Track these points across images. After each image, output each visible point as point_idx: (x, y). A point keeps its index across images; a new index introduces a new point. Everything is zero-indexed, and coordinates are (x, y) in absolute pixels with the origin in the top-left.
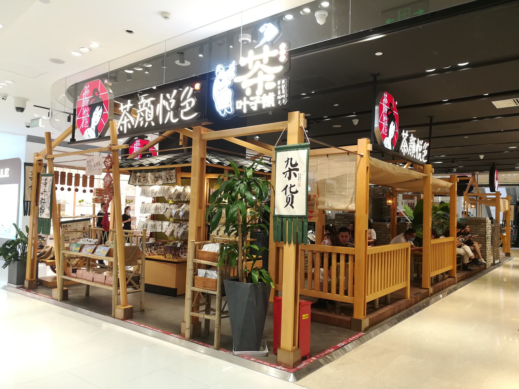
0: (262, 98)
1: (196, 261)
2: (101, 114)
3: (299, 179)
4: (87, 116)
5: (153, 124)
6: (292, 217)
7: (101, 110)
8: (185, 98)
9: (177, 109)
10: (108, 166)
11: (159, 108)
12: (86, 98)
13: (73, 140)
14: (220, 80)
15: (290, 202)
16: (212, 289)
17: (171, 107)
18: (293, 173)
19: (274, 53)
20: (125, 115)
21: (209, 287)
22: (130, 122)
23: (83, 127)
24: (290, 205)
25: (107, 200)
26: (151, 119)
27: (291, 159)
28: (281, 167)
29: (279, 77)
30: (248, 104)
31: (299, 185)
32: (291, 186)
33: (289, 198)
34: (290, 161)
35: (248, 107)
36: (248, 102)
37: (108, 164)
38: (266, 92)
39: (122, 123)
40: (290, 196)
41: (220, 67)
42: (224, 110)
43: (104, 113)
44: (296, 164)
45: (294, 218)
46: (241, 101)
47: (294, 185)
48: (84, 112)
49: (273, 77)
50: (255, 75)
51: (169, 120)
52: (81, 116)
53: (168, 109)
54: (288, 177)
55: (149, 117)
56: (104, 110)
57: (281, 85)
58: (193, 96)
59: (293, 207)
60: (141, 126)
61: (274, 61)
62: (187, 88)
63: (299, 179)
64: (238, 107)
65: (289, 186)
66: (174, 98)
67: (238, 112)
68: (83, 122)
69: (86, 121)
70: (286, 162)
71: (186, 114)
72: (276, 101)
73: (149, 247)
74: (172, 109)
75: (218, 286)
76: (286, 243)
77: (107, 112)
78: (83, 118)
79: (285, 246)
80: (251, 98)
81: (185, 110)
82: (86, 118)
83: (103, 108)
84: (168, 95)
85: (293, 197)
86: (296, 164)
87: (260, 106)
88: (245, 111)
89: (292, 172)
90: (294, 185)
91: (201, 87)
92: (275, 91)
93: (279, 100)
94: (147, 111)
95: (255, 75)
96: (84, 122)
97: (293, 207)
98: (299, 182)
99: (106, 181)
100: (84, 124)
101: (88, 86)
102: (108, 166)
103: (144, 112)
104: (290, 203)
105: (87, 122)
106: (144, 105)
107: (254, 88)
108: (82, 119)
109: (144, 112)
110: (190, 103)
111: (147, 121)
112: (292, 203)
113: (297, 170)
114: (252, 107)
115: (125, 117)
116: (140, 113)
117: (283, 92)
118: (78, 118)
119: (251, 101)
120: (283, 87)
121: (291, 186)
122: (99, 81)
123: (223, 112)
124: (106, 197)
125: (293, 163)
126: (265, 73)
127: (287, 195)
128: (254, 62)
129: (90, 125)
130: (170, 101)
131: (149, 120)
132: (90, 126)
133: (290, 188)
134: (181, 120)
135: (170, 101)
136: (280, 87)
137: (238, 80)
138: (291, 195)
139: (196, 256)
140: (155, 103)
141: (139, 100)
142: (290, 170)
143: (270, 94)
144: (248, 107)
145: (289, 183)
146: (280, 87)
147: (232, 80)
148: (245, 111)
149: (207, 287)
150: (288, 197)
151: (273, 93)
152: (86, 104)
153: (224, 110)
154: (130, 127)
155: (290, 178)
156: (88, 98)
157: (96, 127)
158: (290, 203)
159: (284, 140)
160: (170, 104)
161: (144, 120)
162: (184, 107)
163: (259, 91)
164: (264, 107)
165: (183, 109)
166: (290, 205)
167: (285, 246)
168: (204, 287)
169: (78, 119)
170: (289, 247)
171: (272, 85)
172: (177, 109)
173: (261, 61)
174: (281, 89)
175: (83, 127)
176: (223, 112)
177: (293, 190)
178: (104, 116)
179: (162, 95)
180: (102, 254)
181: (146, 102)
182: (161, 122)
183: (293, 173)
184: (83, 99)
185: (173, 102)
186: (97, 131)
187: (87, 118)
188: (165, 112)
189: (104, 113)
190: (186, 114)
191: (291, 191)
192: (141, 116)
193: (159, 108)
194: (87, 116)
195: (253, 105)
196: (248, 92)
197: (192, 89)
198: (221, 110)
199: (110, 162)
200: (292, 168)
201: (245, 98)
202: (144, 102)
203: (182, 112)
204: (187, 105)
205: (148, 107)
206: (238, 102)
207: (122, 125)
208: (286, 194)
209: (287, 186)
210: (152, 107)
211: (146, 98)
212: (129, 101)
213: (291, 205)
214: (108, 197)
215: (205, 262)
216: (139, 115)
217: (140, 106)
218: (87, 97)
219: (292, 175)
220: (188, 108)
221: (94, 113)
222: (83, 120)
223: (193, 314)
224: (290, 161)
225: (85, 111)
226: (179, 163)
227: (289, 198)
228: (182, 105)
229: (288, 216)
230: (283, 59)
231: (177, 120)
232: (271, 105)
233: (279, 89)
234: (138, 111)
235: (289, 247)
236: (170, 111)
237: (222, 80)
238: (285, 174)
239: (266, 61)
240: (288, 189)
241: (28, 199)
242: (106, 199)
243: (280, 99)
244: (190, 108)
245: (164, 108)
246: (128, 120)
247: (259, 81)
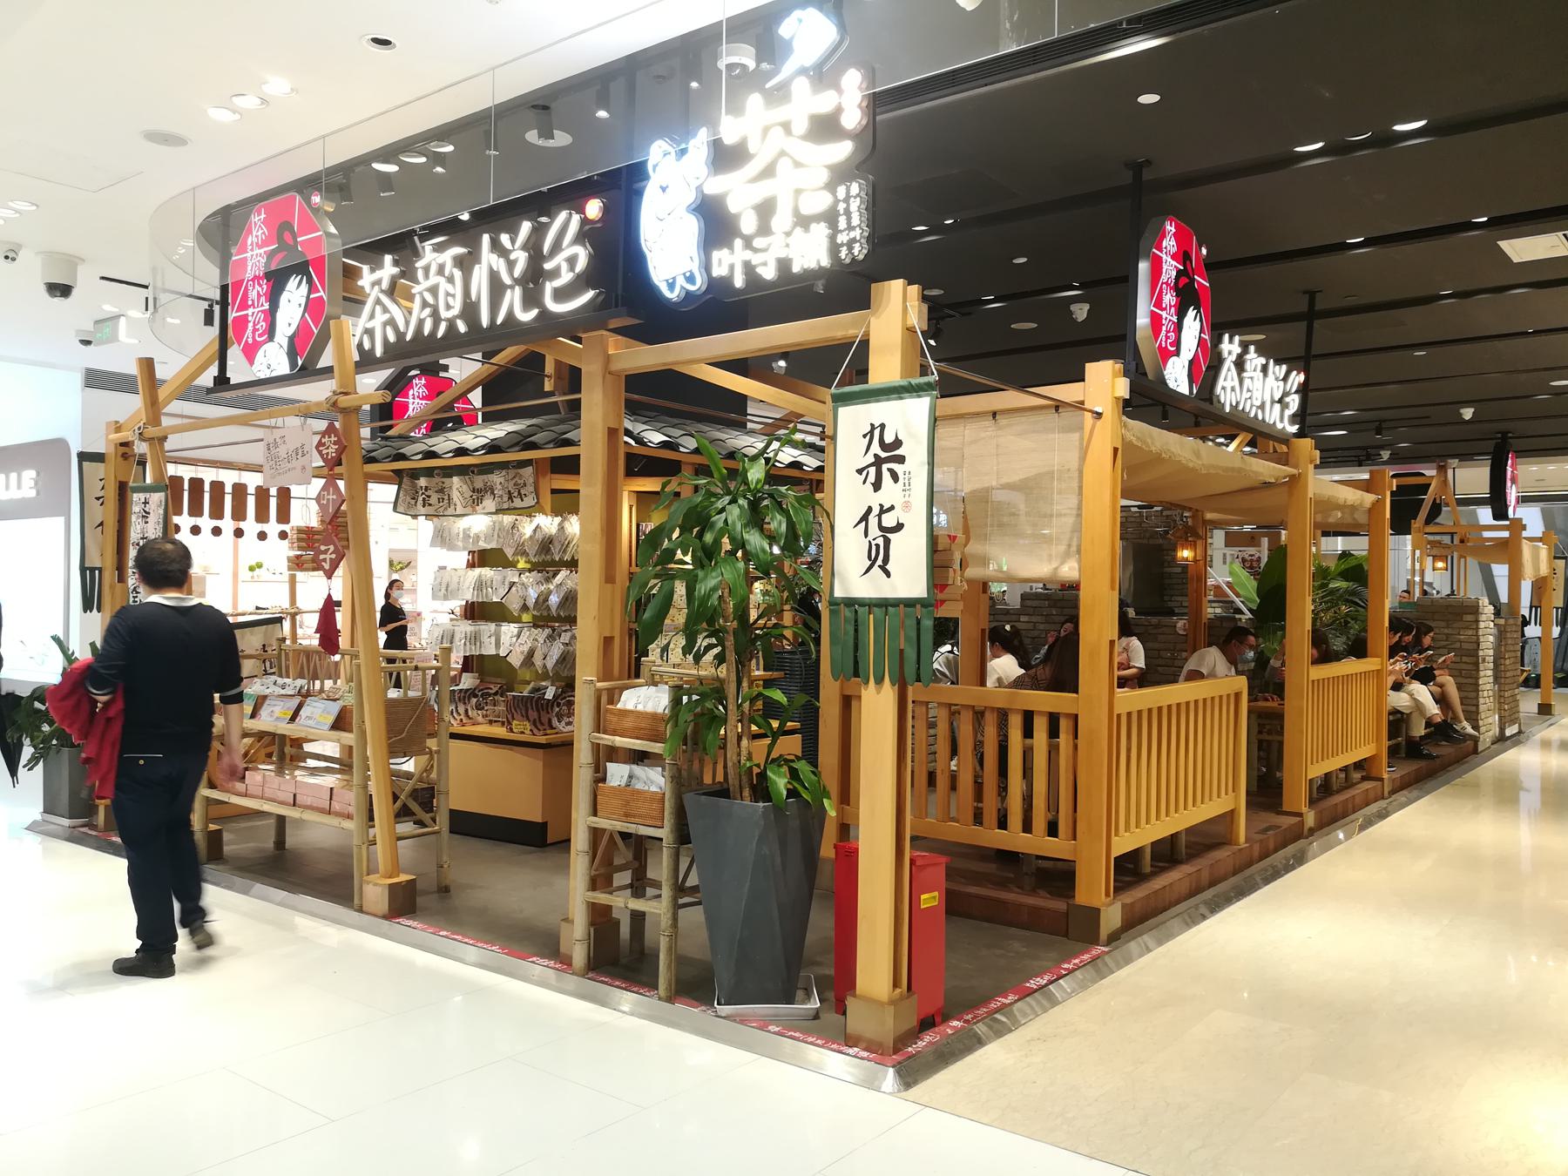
0: (789, 240)
1: (602, 739)
2: (303, 301)
3: (907, 487)
4: (262, 305)
5: (462, 327)
6: (884, 604)
7: (304, 288)
8: (557, 247)
9: (534, 278)
10: (329, 457)
11: (480, 277)
12: (257, 251)
13: (222, 381)
14: (661, 187)
15: (879, 558)
16: (650, 823)
17: (517, 272)
18: (889, 469)
19: (825, 102)
20: (378, 302)
21: (640, 816)
22: (391, 322)
23: (250, 341)
24: (879, 566)
25: (328, 561)
26: (456, 311)
27: (883, 426)
28: (850, 453)
29: (840, 175)
30: (748, 259)
31: (907, 506)
32: (883, 511)
33: (878, 546)
34: (877, 432)
35: (749, 268)
36: (748, 255)
37: (330, 450)
38: (804, 222)
39: (369, 325)
40: (880, 541)
41: (663, 149)
42: (674, 278)
43: (312, 296)
44: (898, 443)
45: (892, 606)
46: (725, 251)
47: (892, 508)
48: (253, 295)
49: (824, 176)
50: (768, 172)
51: (510, 315)
52: (244, 305)
53: (507, 280)
54: (873, 482)
55: (448, 307)
56: (312, 288)
57: (847, 200)
58: (580, 238)
59: (888, 574)
60: (426, 333)
61: (825, 128)
62: (563, 215)
63: (907, 487)
64: (718, 271)
65: (876, 510)
66: (524, 247)
67: (718, 287)
68: (251, 325)
70: (865, 436)
71: (560, 295)
72: (834, 248)
73: (460, 700)
74: (517, 281)
75: (666, 813)
76: (867, 682)
77: (322, 293)
78: (250, 311)
79: (866, 690)
80: (758, 243)
81: (558, 283)
82: (258, 312)
83: (310, 282)
84: (505, 239)
85: (887, 542)
86: (898, 443)
87: (784, 264)
88: (739, 282)
89: (885, 467)
90: (892, 508)
91: (606, 210)
92: (830, 217)
93: (842, 245)
94: (444, 286)
95: (768, 172)
96: (254, 325)
97: (888, 574)
98: (907, 499)
99: (325, 502)
100: (255, 330)
101: (263, 216)
102: (329, 457)
103: (434, 290)
104: (879, 562)
105: (264, 324)
106: (433, 269)
107: (765, 210)
108: (247, 315)
109: (434, 290)
110: (572, 261)
111: (443, 318)
112: (886, 560)
113: (901, 460)
114: (759, 270)
115: (378, 308)
116: (421, 293)
117: (856, 221)
118: (234, 315)
119: (756, 250)
120: (855, 205)
121: (883, 511)
122: (295, 197)
123: (671, 286)
124: (325, 552)
125: (889, 439)
126: (797, 164)
127: (870, 537)
128: (766, 130)
129: (271, 333)
130: (512, 257)
132: (271, 338)
133: (879, 516)
134: (544, 314)
135: (512, 257)
136: (845, 205)
137: (716, 185)
138: (882, 538)
139: (598, 728)
140: (465, 264)
141: (417, 254)
142: (878, 462)
143: (813, 226)
144: (749, 268)
145: (875, 500)
146: (845, 205)
147: (699, 189)
148: (739, 282)
149: (634, 817)
150: (873, 543)
151: (823, 225)
153: (674, 278)
154: (392, 338)
155: (877, 486)
156: (262, 251)
157: (292, 339)
158: (879, 562)
159: (861, 373)
160: (511, 265)
162: (555, 273)
163: (782, 220)
164: (796, 269)
165: (550, 280)
166: (879, 566)
167: (866, 690)
168: (626, 815)
170: (878, 693)
171: (822, 202)
172: (534, 278)
173: (786, 127)
174: (848, 213)
175: (250, 341)
176: (671, 286)
177: (889, 520)
178: (313, 307)
179: (486, 238)
180: (318, 723)
181: (440, 261)
182: (485, 322)
183: (889, 469)
184: (249, 255)
185: (521, 258)
186: (292, 353)
187: (263, 311)
189: (312, 296)
190: (560, 295)
191: (884, 524)
192: (425, 304)
193: (480, 277)
194: (262, 305)
195: (765, 264)
196: (748, 224)
197: (576, 218)
198: (667, 281)
199: (337, 447)
200: (883, 455)
201: (738, 243)
202: (434, 259)
203: (549, 287)
204: (564, 267)
205: (444, 276)
206: (717, 255)
207: (369, 332)
208: (866, 536)
209: (870, 510)
210: (458, 274)
211: (439, 248)
212: (388, 258)
213: (883, 568)
214: (330, 552)
215: (630, 743)
216: (418, 299)
217: (420, 274)
218: (259, 247)
219: (886, 476)
220: (566, 277)
222: (250, 318)
223: (594, 898)
224: (877, 432)
225: (256, 292)
226: (413, 455)
227: (878, 546)
228: (548, 266)
229: (874, 602)
230: (853, 118)
231: (534, 312)
232: (818, 262)
233: (842, 212)
234: (416, 289)
235: (878, 693)
236: (512, 287)
237: (667, 187)
238: (865, 473)
239: (801, 126)
240: (873, 520)
241: (94, 561)
242: (328, 557)
243: (845, 242)
244: (571, 275)
245: (494, 277)
246: (387, 316)
247: (780, 188)
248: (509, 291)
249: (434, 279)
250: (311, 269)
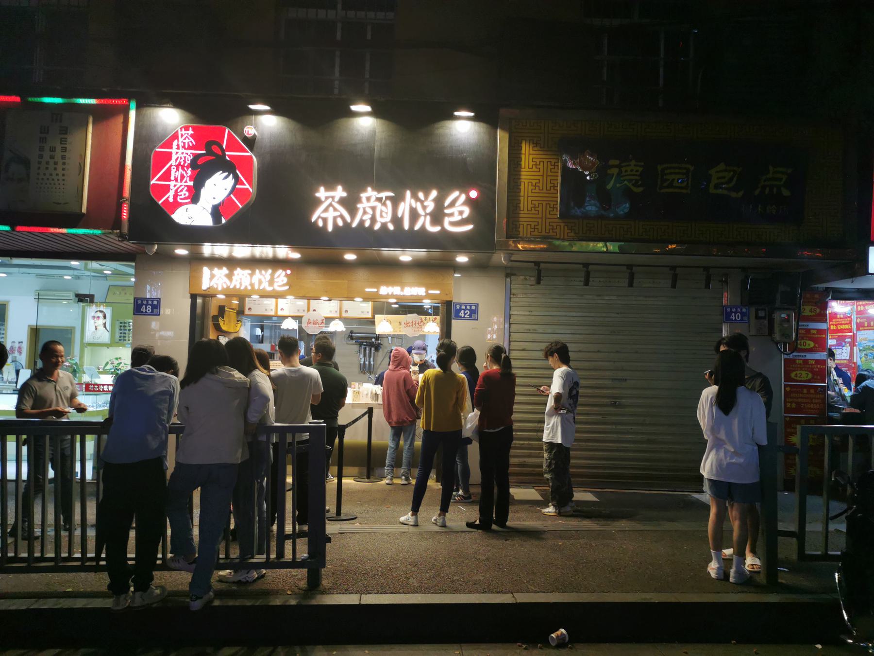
7: (230, 181)
23: (171, 200)
56: (237, 181)
69: (181, 191)
78: (172, 184)
82: (181, 186)
83: (236, 178)
105: (187, 194)
108: (169, 185)
118: (153, 182)
131: (383, 220)
152: (185, 162)
169: (153, 184)
175: (171, 200)
187: (185, 186)
221: (209, 183)
222: (172, 187)
250: (237, 172)
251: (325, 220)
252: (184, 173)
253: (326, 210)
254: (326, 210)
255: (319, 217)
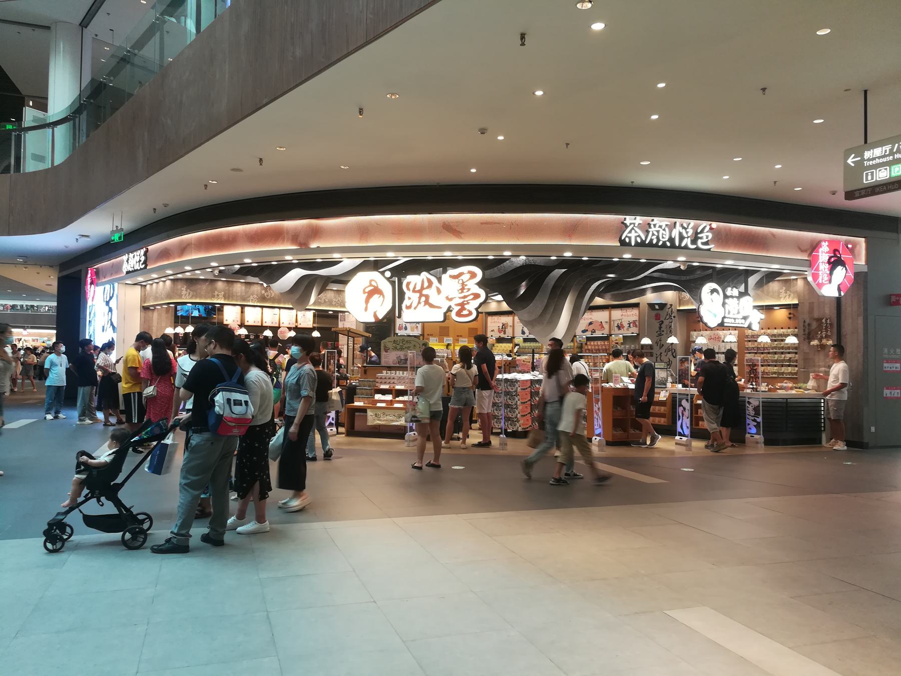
5: (668, 244)
8: (702, 232)
17: (689, 234)
26: (666, 239)
53: (686, 236)
55: (663, 238)
71: (703, 244)
94: (661, 231)
103: (658, 232)
116: (652, 231)
160: (687, 233)
161: (658, 238)
162: (701, 238)
188: (682, 238)
190: (703, 244)
204: (705, 237)
220: (705, 240)
236: (688, 237)
245: (680, 234)
248: (686, 239)
249: (657, 229)
251: (630, 238)
252: (684, 232)
253: (630, 232)
254: (630, 232)
255: (626, 236)
